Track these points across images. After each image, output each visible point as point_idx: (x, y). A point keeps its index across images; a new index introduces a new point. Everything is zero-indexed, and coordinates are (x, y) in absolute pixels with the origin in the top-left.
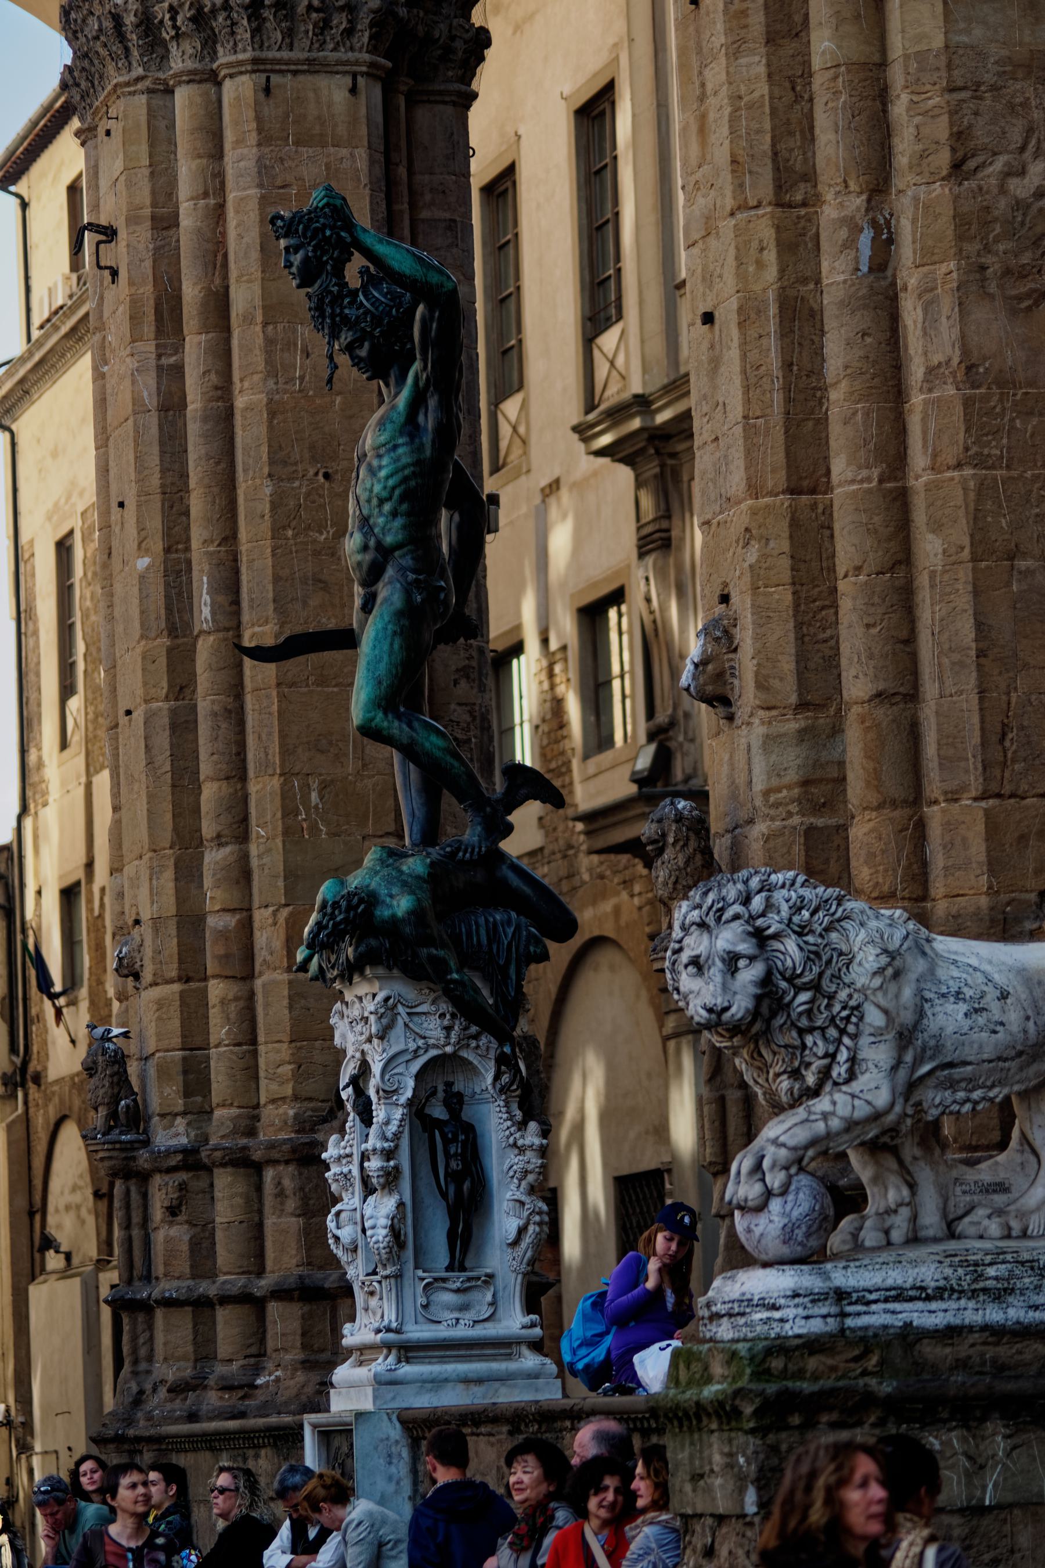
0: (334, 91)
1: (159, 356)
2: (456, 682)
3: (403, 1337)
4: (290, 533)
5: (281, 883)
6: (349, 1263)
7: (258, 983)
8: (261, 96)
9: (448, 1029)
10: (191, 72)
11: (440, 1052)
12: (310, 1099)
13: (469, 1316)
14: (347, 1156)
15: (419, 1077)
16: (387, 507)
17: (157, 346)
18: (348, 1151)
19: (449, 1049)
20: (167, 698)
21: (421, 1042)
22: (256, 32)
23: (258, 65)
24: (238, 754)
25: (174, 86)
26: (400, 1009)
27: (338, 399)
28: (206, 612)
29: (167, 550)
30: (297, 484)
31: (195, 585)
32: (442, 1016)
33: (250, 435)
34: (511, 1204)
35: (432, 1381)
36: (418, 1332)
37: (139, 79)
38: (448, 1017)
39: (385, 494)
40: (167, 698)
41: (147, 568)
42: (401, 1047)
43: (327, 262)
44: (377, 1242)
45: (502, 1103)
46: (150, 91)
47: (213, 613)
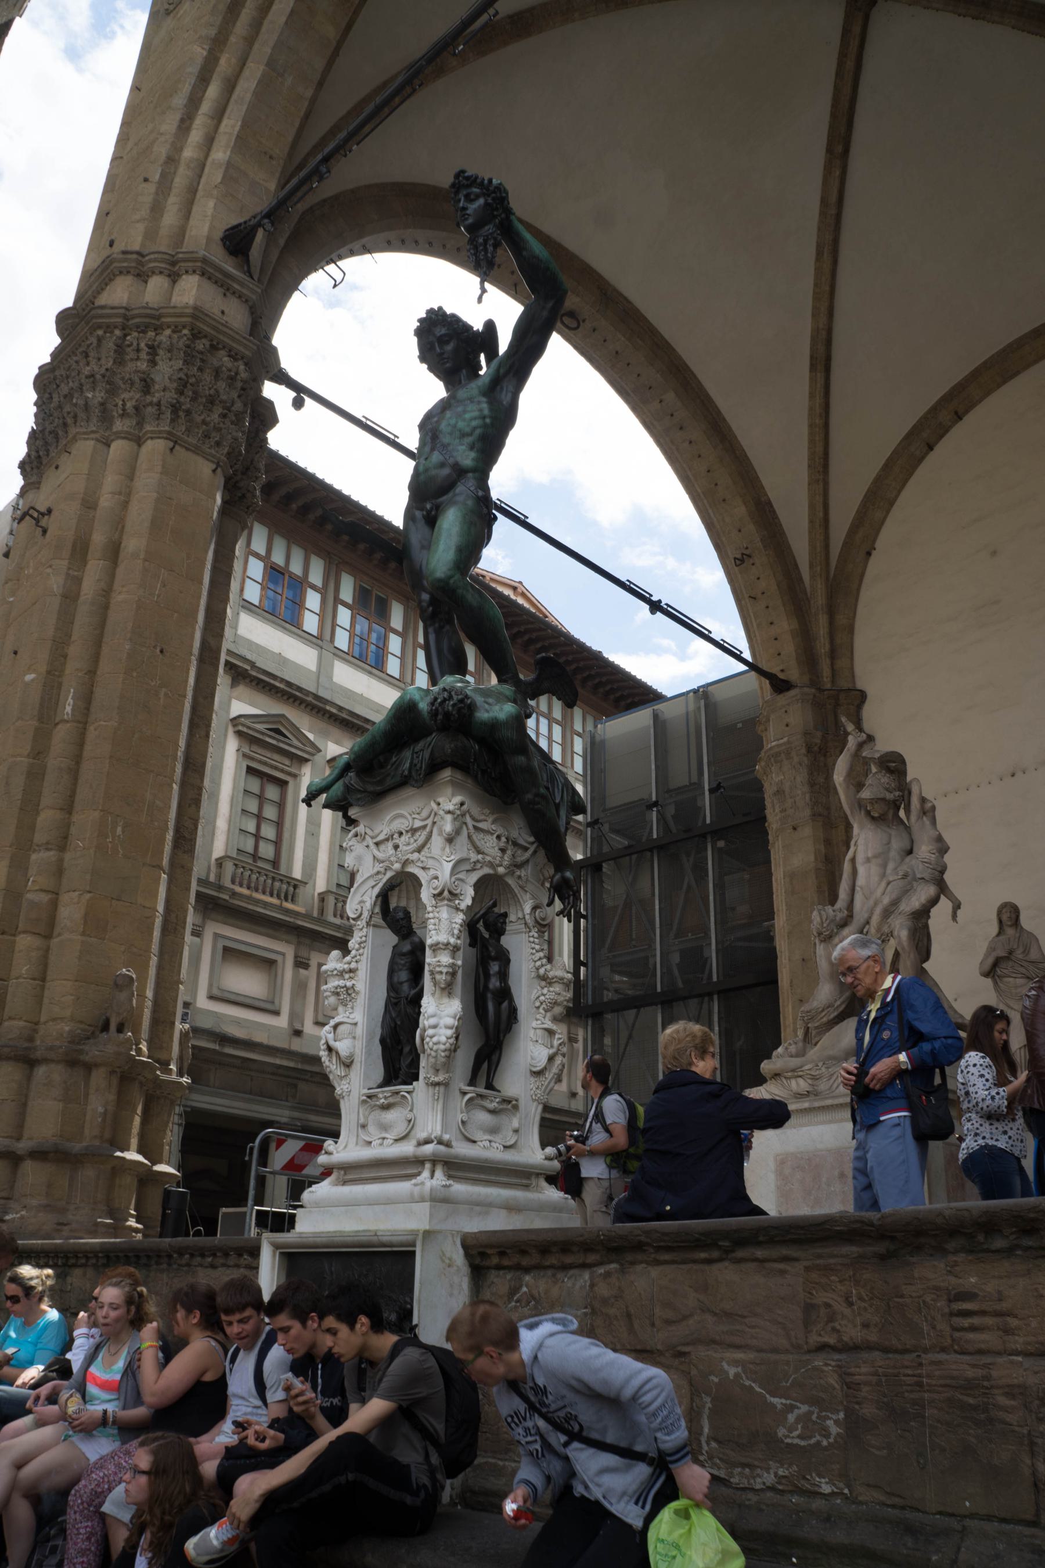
0: (204, 468)
1: (69, 569)
2: (190, 806)
3: (452, 1151)
4: (135, 674)
5: (88, 877)
6: (341, 1078)
7: (55, 941)
8: (168, 452)
9: (503, 851)
10: (127, 432)
11: (491, 872)
12: (81, 1022)
13: (499, 1140)
14: (351, 971)
15: (477, 886)
16: (468, 440)
17: (69, 563)
18: (353, 965)
19: (501, 870)
20: (28, 756)
21: (480, 857)
22: (173, 421)
23: (170, 436)
24: (70, 796)
25: (113, 440)
26: (468, 819)
27: (176, 615)
28: (68, 709)
29: (49, 672)
30: (144, 649)
31: (62, 694)
32: (499, 837)
33: (121, 617)
34: (539, 1032)
35: (478, 1204)
36: (462, 1149)
37: (93, 432)
38: (503, 839)
39: (467, 430)
40: (28, 756)
41: (33, 680)
42: (464, 855)
43: (495, 217)
44: (438, 1043)
45: (536, 935)
46: (97, 440)
47: (72, 710)
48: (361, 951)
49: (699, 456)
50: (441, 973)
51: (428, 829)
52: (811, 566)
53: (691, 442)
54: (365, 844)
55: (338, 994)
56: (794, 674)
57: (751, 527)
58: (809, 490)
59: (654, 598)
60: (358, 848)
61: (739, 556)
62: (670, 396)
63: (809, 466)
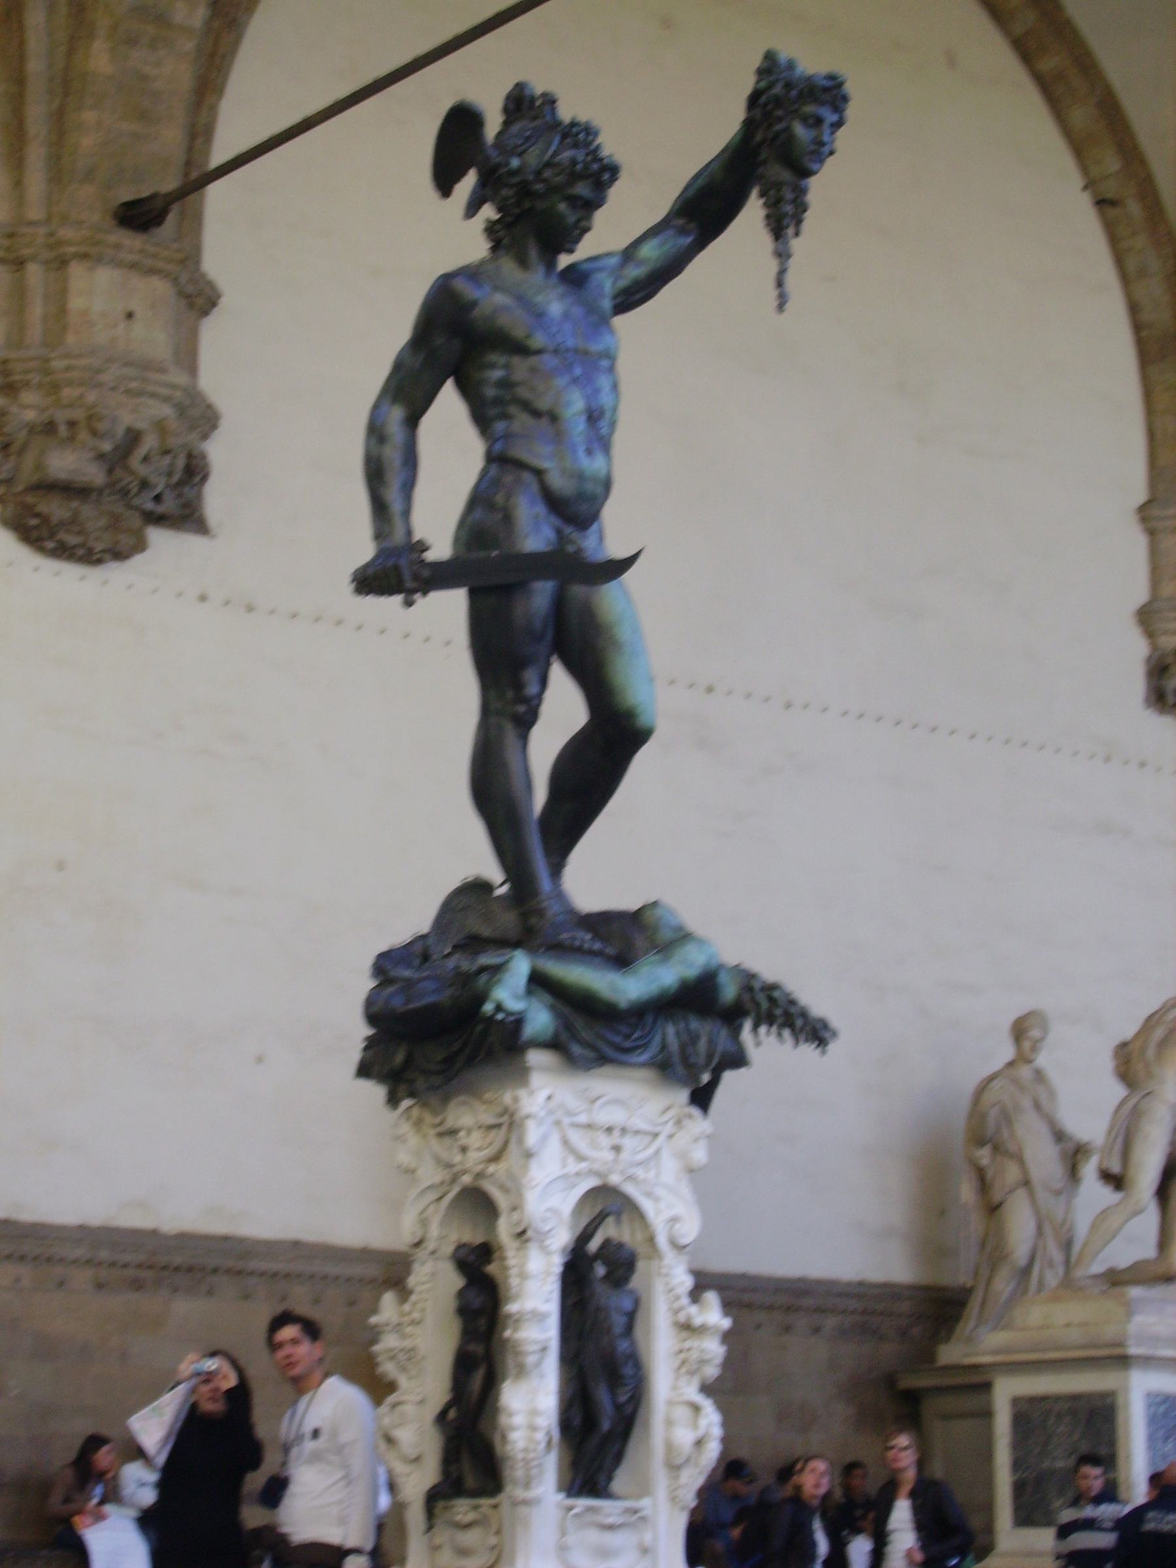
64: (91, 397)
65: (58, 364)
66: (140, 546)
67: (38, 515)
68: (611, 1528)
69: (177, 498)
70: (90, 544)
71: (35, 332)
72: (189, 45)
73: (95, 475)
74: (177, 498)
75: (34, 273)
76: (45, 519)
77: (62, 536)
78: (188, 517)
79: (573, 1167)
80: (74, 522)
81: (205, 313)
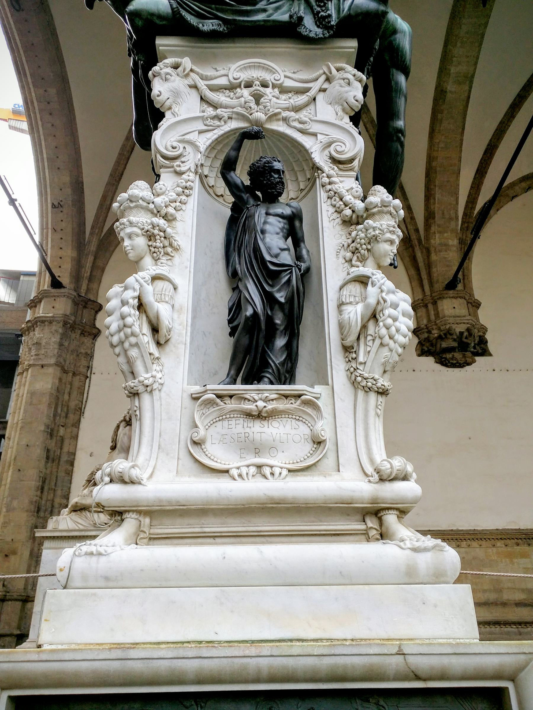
18: (171, 210)
48: (183, 198)
49: (55, 136)
50: (392, 242)
51: (311, 93)
52: (93, 228)
53: (53, 125)
54: (189, 81)
55: (151, 237)
56: (65, 280)
57: (69, 191)
58: (105, 187)
59: (13, 197)
60: (178, 83)
61: (56, 204)
62: (52, 91)
63: (111, 175)
64: (448, 327)
65: (438, 322)
66: (474, 361)
67: (444, 358)
68: (260, 416)
69: (482, 349)
70: (459, 362)
71: (433, 318)
72: (455, 249)
73: (455, 344)
74: (482, 349)
75: (430, 306)
76: (446, 358)
77: (451, 361)
78: (485, 352)
79: (210, 111)
80: (453, 358)
81: (478, 308)
